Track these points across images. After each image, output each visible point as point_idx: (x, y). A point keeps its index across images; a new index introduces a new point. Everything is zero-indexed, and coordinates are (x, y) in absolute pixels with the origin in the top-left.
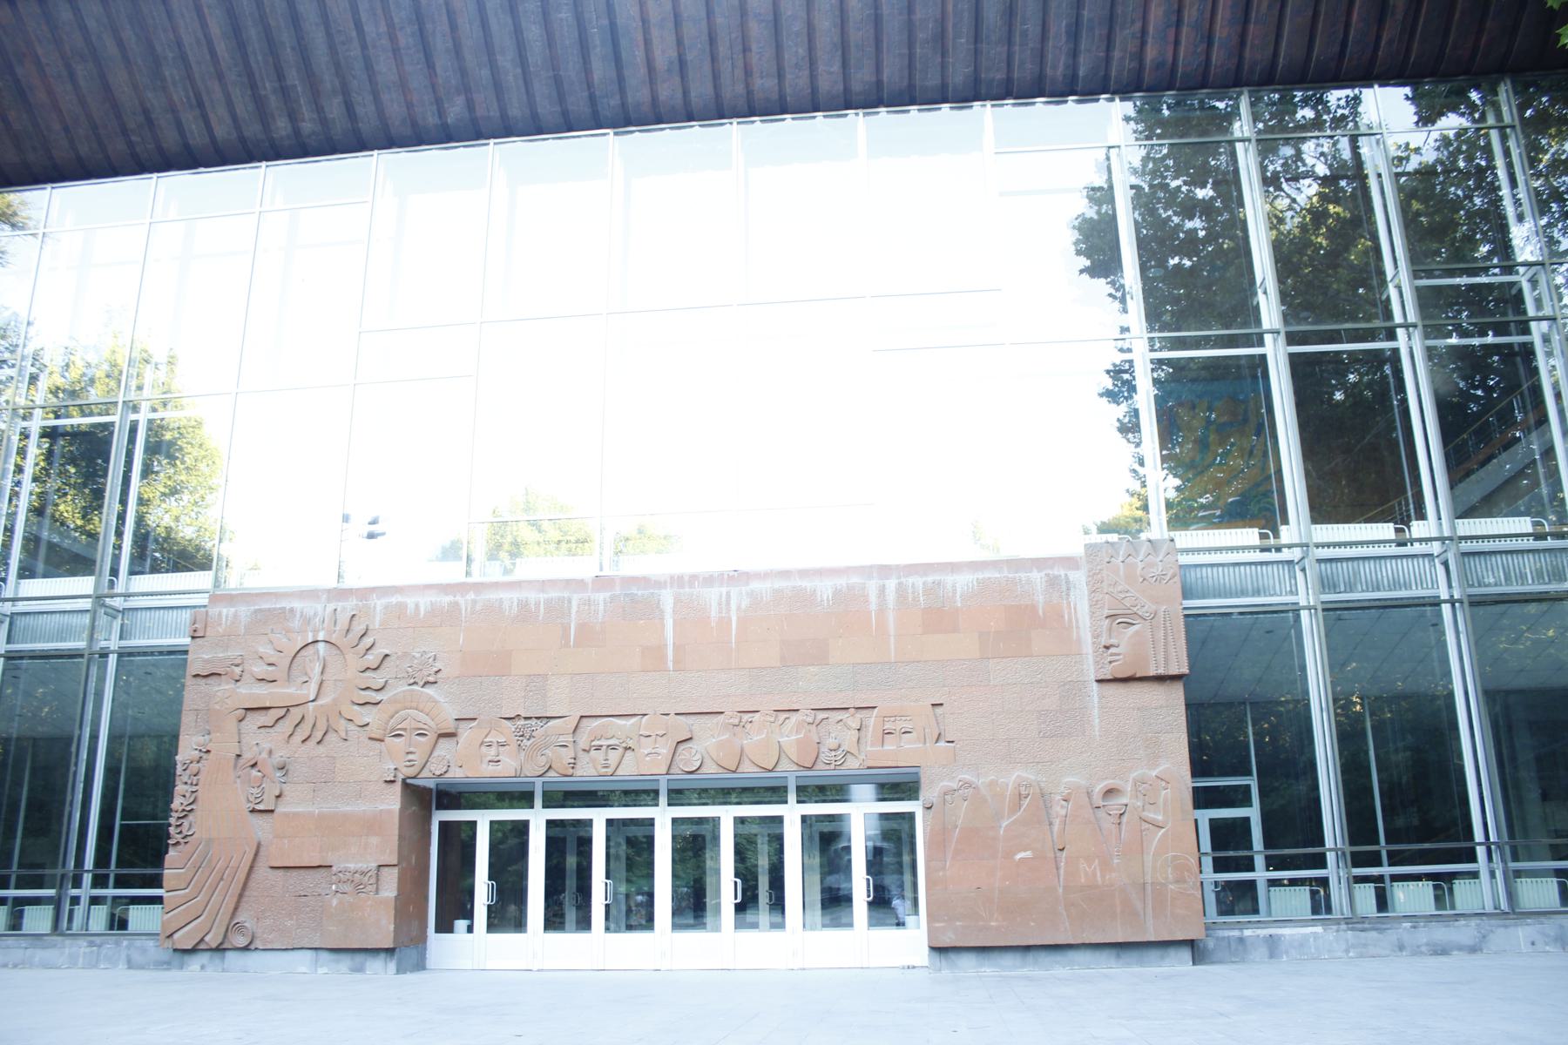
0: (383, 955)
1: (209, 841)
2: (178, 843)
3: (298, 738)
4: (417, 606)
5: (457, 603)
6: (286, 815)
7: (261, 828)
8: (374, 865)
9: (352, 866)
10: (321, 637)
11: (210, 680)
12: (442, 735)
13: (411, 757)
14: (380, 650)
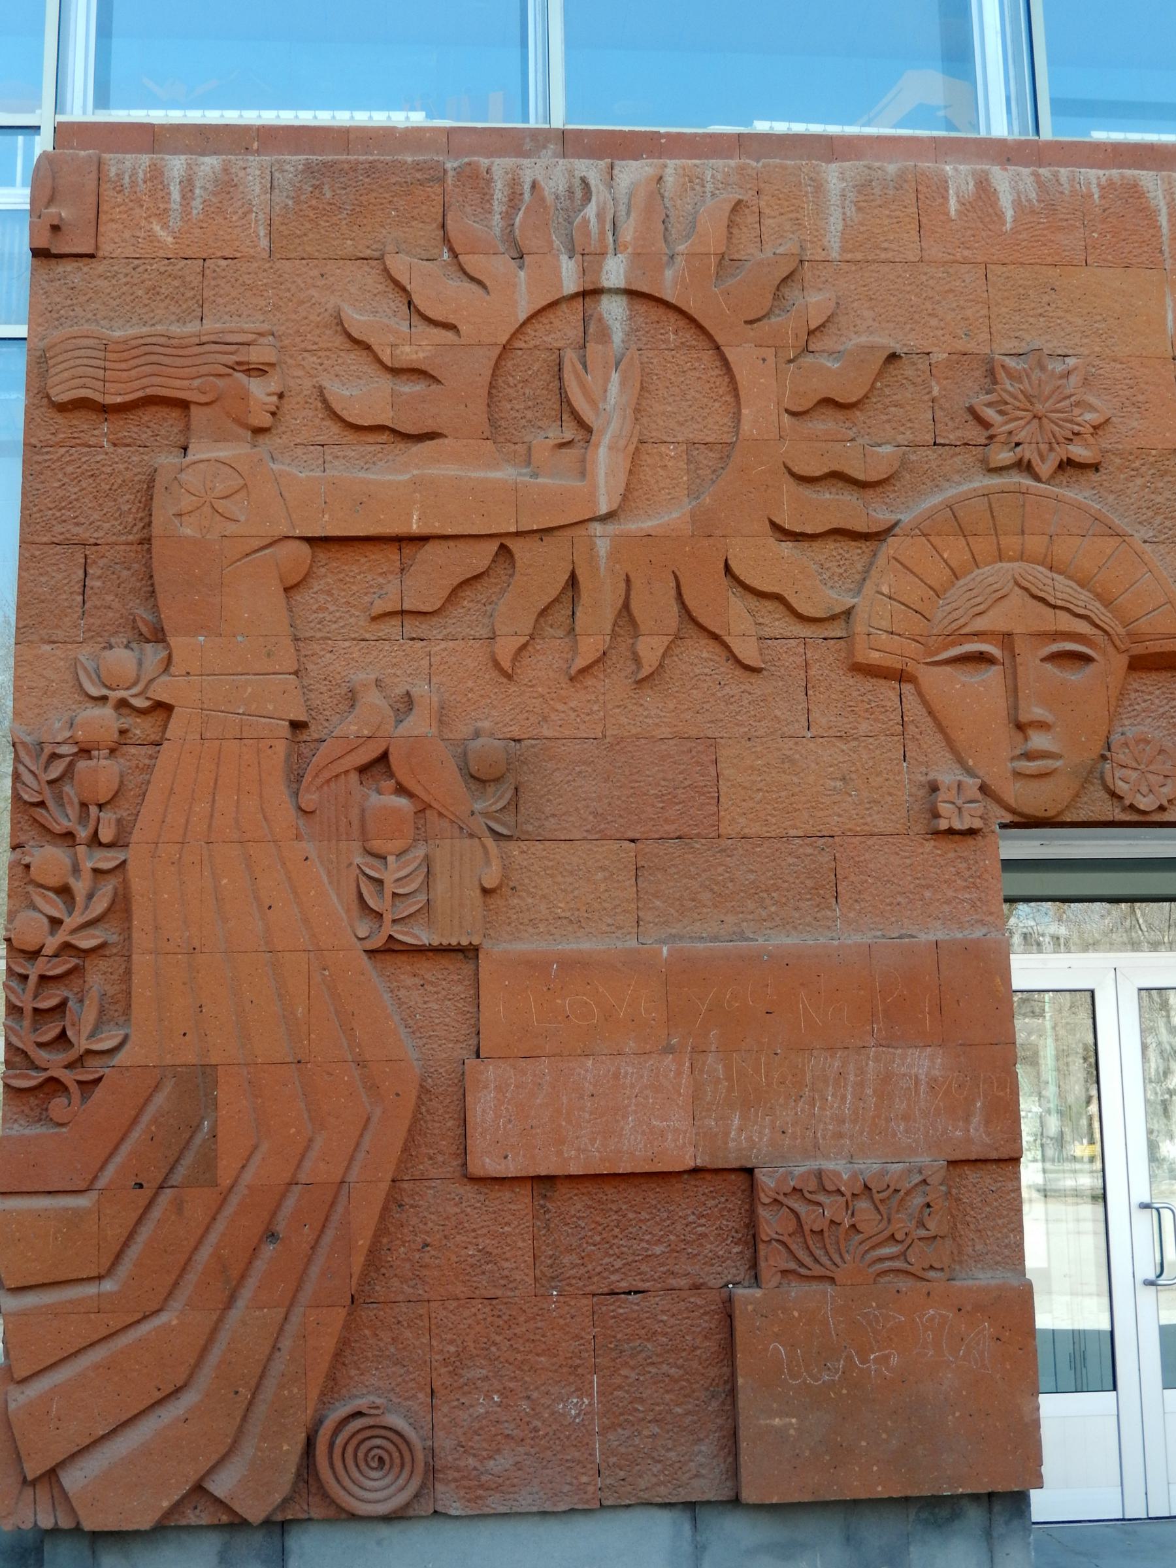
0: (974, 1515)
1: (200, 1082)
2: (53, 1085)
3: (547, 662)
4: (984, 186)
5: (1134, 191)
6: (535, 966)
7: (409, 1020)
8: (931, 1162)
9: (837, 1166)
10: (614, 272)
11: (128, 428)
12: (1140, 664)
13: (1039, 741)
14: (869, 334)
